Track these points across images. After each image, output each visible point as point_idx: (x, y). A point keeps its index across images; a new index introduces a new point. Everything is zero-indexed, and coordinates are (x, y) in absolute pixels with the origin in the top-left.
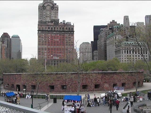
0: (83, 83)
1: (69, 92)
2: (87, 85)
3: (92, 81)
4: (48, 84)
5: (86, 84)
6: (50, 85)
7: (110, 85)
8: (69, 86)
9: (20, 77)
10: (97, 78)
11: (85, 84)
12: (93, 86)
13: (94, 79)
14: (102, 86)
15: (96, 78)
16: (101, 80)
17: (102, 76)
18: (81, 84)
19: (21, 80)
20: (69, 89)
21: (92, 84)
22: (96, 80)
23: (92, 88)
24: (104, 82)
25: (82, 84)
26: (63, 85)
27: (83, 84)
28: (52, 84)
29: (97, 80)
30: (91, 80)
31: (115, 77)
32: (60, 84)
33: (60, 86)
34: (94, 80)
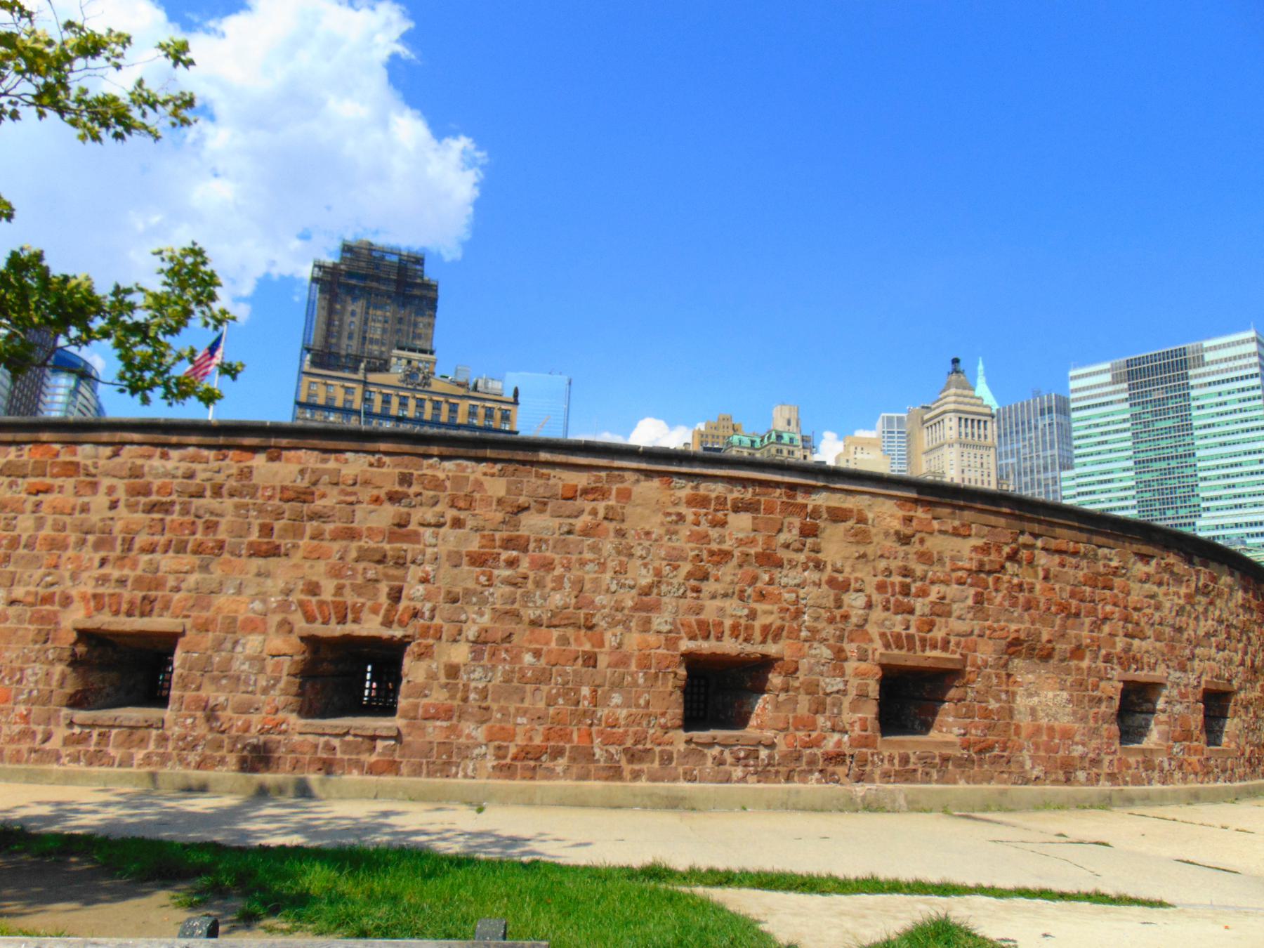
0: (705, 631)
1: (444, 769)
2: (766, 663)
3: (855, 602)
4: (67, 601)
5: (755, 649)
6: (106, 621)
7: (1082, 690)
8: (460, 654)
10: (919, 569)
11: (730, 646)
12: (862, 696)
13: (871, 583)
14: (993, 705)
15: (906, 572)
16: (979, 600)
17: (985, 549)
18: (671, 642)
20: (448, 714)
21: (840, 656)
22: (906, 591)
23: (847, 717)
24: (1015, 646)
25: (686, 645)
26: (351, 628)
27: (706, 646)
28: (146, 607)
29: (921, 605)
30: (832, 582)
31: (1137, 593)
32: (284, 606)
33: (277, 643)
34: (877, 598)
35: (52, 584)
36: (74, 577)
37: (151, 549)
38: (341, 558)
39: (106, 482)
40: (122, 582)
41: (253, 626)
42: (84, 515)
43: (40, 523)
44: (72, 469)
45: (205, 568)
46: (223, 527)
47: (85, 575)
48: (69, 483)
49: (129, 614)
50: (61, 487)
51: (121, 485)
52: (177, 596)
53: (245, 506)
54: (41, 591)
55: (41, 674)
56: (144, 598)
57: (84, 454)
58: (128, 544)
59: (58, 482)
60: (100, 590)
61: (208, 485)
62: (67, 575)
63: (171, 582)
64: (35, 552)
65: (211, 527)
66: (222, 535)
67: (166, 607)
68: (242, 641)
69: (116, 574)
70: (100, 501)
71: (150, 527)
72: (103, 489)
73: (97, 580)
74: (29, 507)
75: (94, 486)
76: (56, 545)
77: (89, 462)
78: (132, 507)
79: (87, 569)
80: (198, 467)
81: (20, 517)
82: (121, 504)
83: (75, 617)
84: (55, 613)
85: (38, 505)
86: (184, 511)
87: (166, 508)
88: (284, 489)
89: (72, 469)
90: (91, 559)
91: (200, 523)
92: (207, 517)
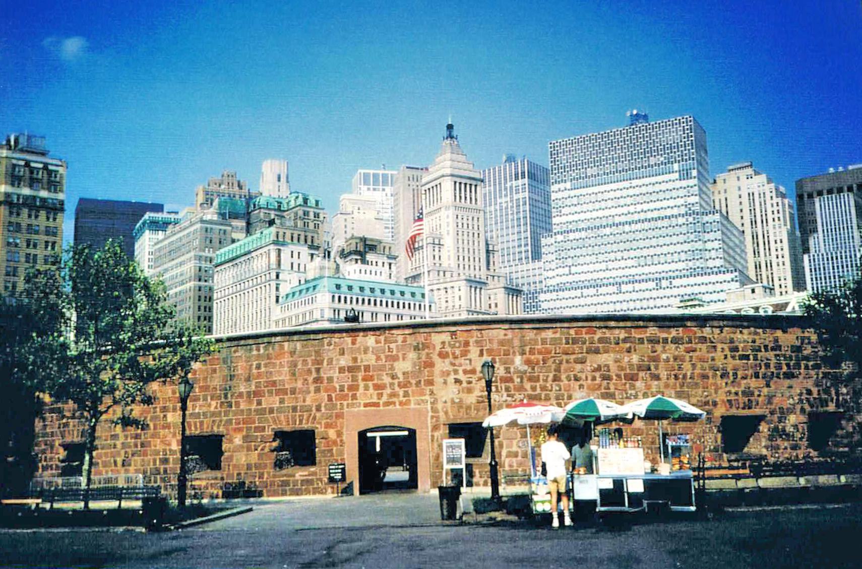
4: (715, 404)
9: (412, 355)
19: (430, 383)
32: (801, 401)
35: (707, 396)
36: (716, 393)
37: (744, 378)
38: (817, 378)
39: (719, 346)
40: (736, 394)
41: (791, 411)
42: (713, 363)
43: (694, 366)
44: (703, 340)
45: (768, 386)
46: (772, 366)
47: (720, 392)
48: (704, 347)
49: (744, 408)
50: (700, 349)
51: (726, 346)
52: (760, 399)
53: (778, 355)
54: (704, 400)
55: (713, 438)
56: (749, 400)
57: (707, 331)
58: (735, 374)
59: (699, 346)
60: (729, 398)
61: (762, 346)
62: (713, 391)
63: (757, 393)
64: (695, 381)
65: (767, 366)
66: (773, 370)
67: (757, 404)
68: (788, 418)
69: (733, 391)
70: (719, 355)
71: (743, 367)
72: (719, 349)
73: (726, 393)
74: (687, 358)
75: (715, 347)
76: (705, 377)
77: (711, 336)
78: (733, 357)
79: (721, 388)
80: (757, 337)
81: (685, 364)
82: (729, 356)
83: (720, 411)
84: (712, 410)
85: (691, 357)
86: (756, 359)
87: (747, 357)
88: (792, 346)
89: (703, 340)
90: (721, 384)
91: (763, 364)
92: (766, 361)
